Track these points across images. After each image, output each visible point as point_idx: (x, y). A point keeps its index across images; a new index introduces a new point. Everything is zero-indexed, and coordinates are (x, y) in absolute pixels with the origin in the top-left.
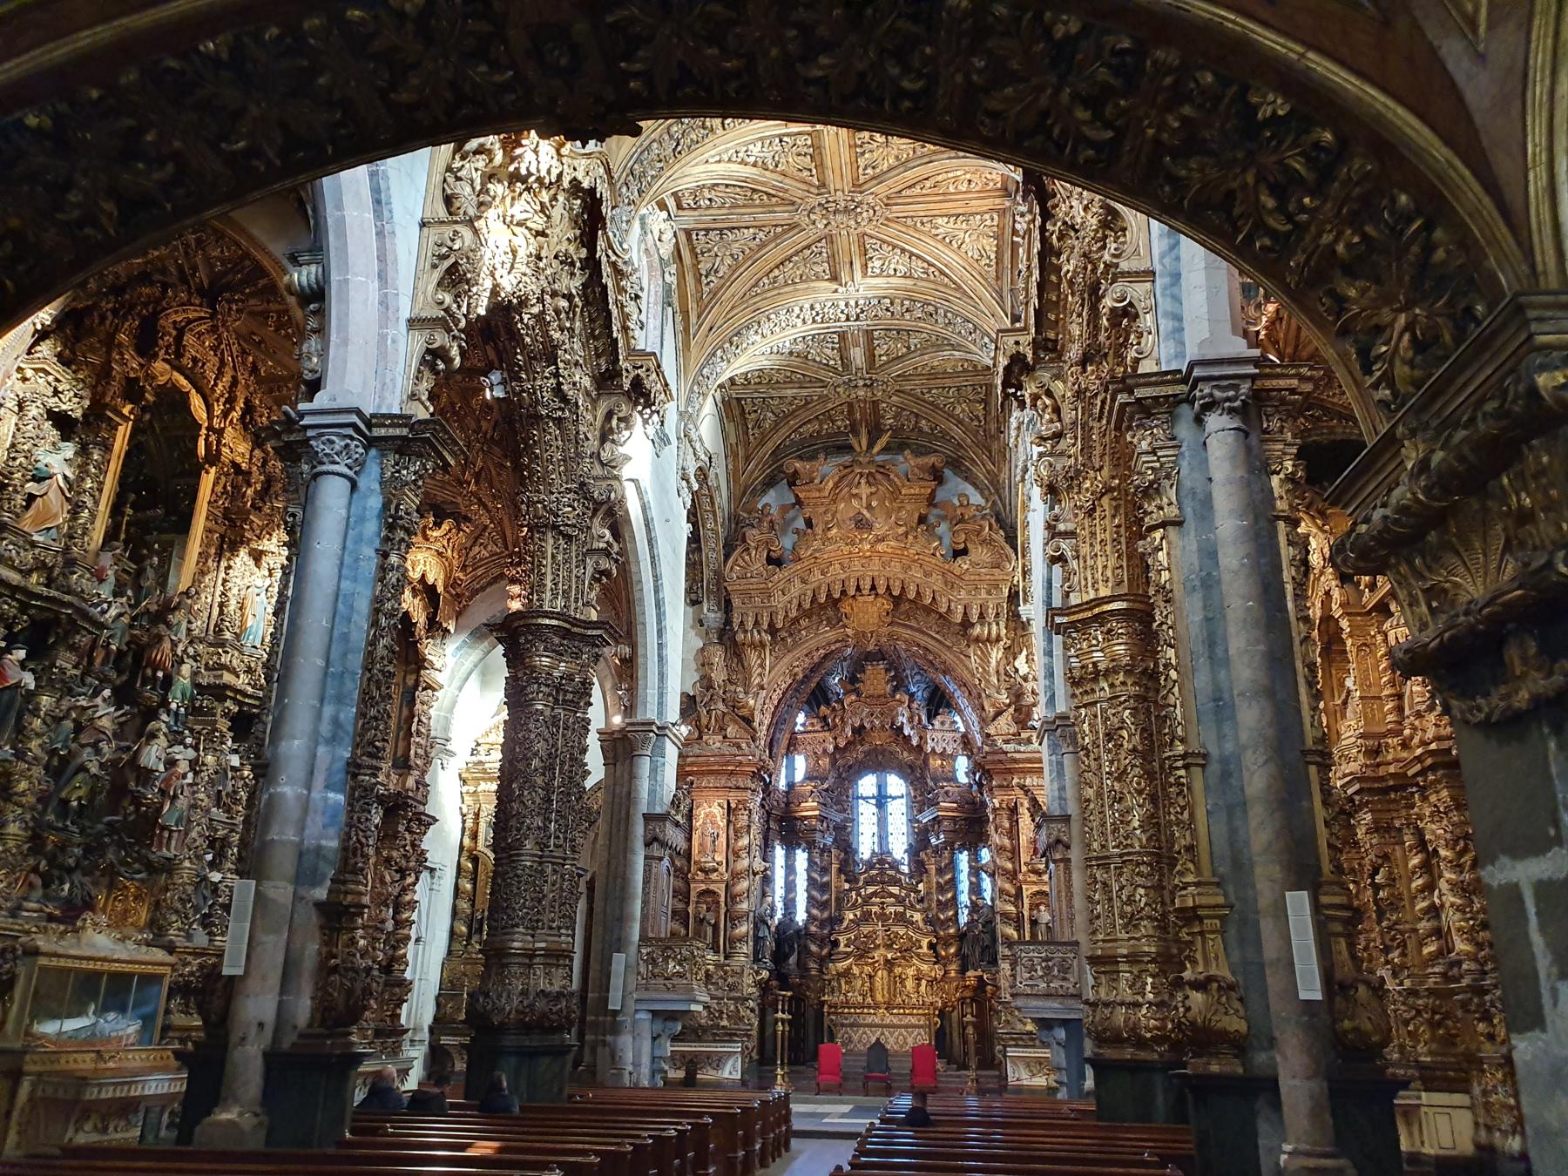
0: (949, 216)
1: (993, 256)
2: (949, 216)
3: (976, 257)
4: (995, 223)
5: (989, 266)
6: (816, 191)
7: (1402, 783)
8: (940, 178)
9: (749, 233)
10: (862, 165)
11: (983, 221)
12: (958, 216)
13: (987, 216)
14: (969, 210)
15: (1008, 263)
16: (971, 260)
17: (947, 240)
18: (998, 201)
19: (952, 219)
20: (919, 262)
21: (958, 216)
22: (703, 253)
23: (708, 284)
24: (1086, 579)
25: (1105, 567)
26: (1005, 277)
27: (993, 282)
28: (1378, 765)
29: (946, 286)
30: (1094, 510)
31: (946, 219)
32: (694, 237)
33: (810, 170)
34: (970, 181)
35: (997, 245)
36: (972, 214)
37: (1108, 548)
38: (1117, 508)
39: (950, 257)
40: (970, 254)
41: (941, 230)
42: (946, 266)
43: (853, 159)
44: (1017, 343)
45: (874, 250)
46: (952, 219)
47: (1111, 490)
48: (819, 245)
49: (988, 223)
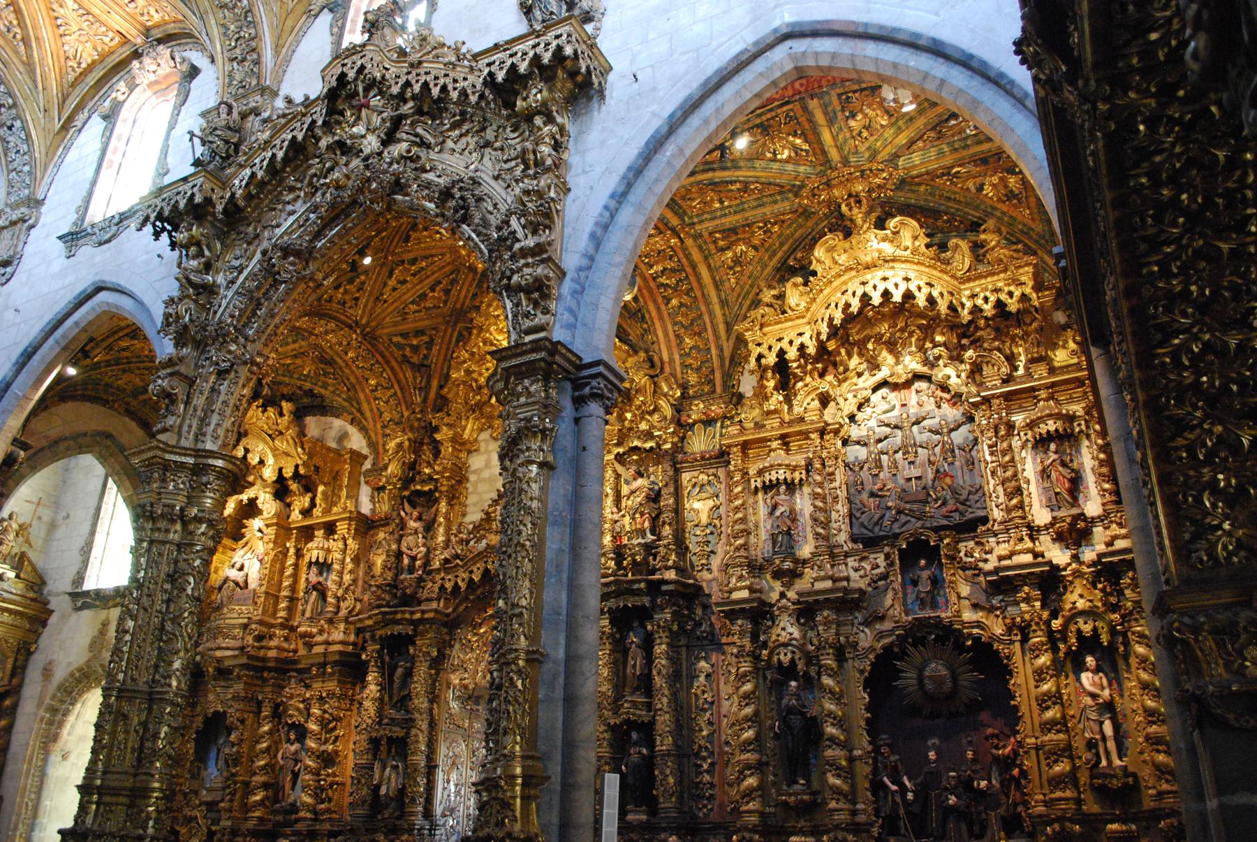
0: (81, 7)
1: (84, 65)
2: (81, 7)
4: (111, 44)
5: (74, 70)
7: (286, 668)
12: (89, 13)
13: (111, 34)
14: (104, 17)
15: (91, 79)
16: (62, 53)
17: (59, 22)
18: (135, 32)
19: (81, 12)
20: (12, 17)
21: (89, 13)
24: (190, 426)
25: (218, 425)
26: (78, 90)
27: (66, 86)
28: (262, 647)
29: (17, 52)
30: (227, 371)
31: (76, 7)
35: (94, 62)
36: (101, 22)
37: (229, 411)
38: (249, 380)
39: (46, 33)
40: (66, 48)
41: (62, 11)
42: (37, 39)
44: (213, 190)
46: (81, 12)
47: (253, 363)
49: (107, 40)
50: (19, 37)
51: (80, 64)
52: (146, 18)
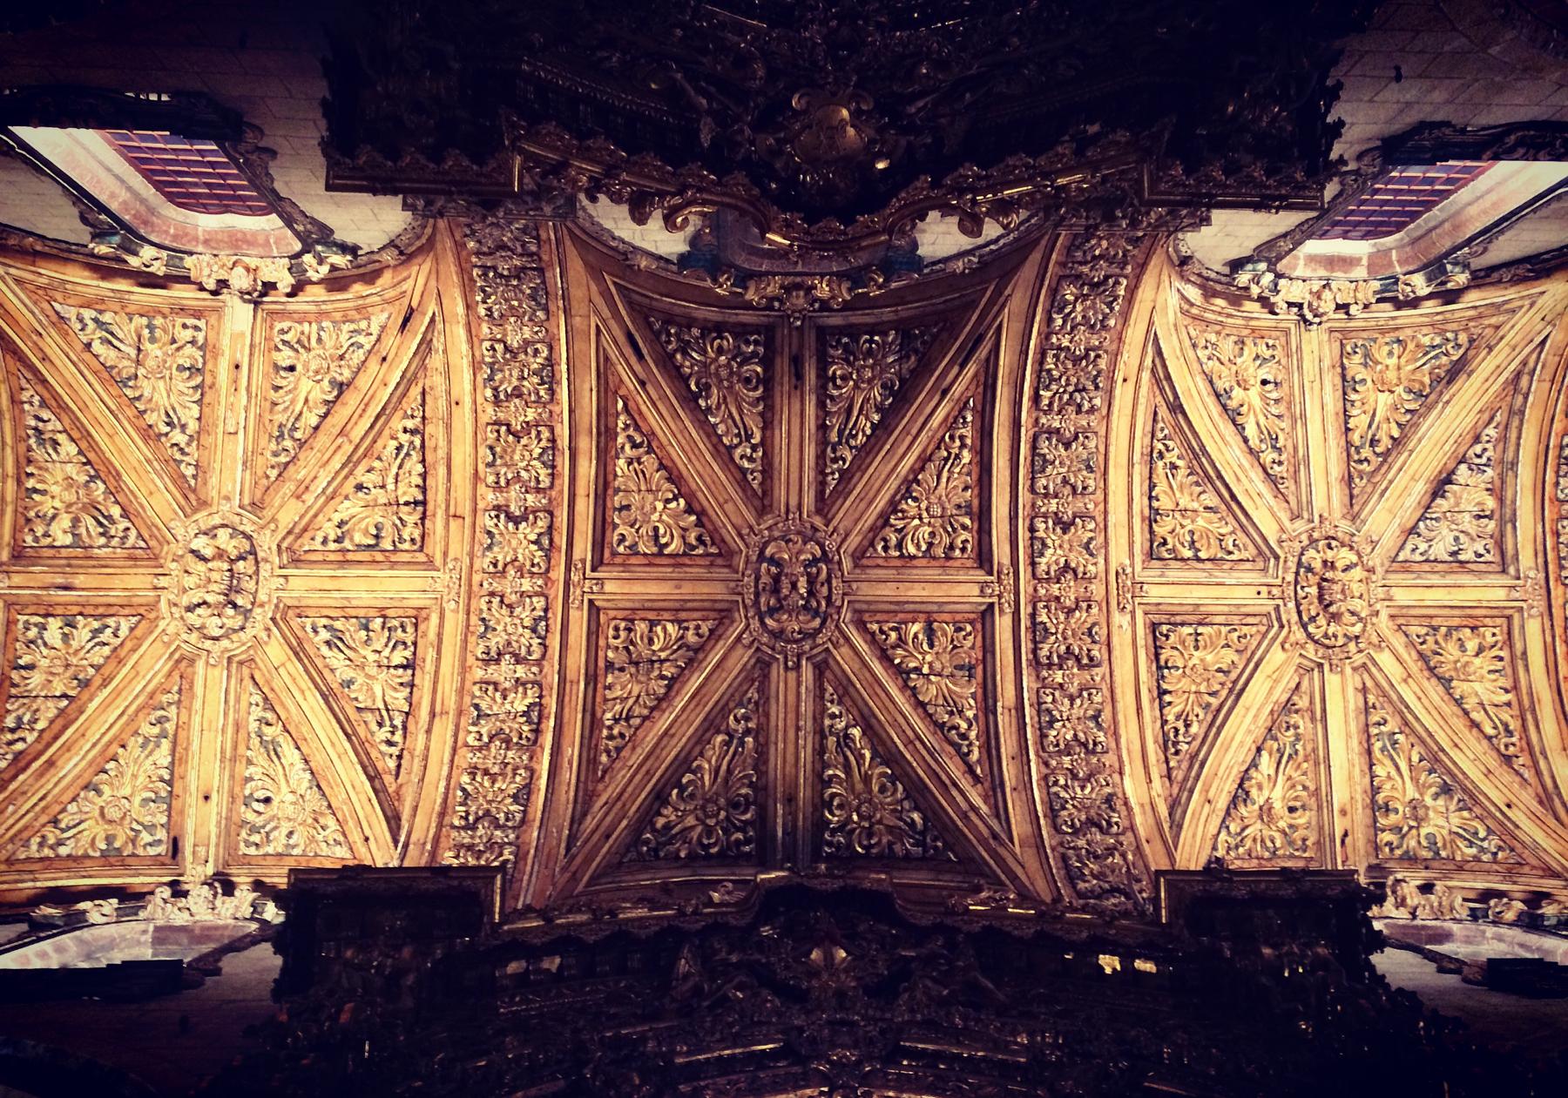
0: (171, 767)
1: (63, 851)
3: (65, 821)
4: (140, 852)
6: (284, 545)
8: (290, 754)
9: (190, 415)
10: (338, 625)
11: (150, 828)
12: (170, 783)
13: (161, 834)
21: (170, 783)
22: (151, 327)
23: (80, 319)
31: (166, 761)
32: (190, 321)
33: (338, 540)
34: (267, 800)
43: (353, 612)
45: (96, 632)
48: (133, 533)
49: (146, 837)
50: (20, 746)
51: (60, 843)
52: (256, 838)
